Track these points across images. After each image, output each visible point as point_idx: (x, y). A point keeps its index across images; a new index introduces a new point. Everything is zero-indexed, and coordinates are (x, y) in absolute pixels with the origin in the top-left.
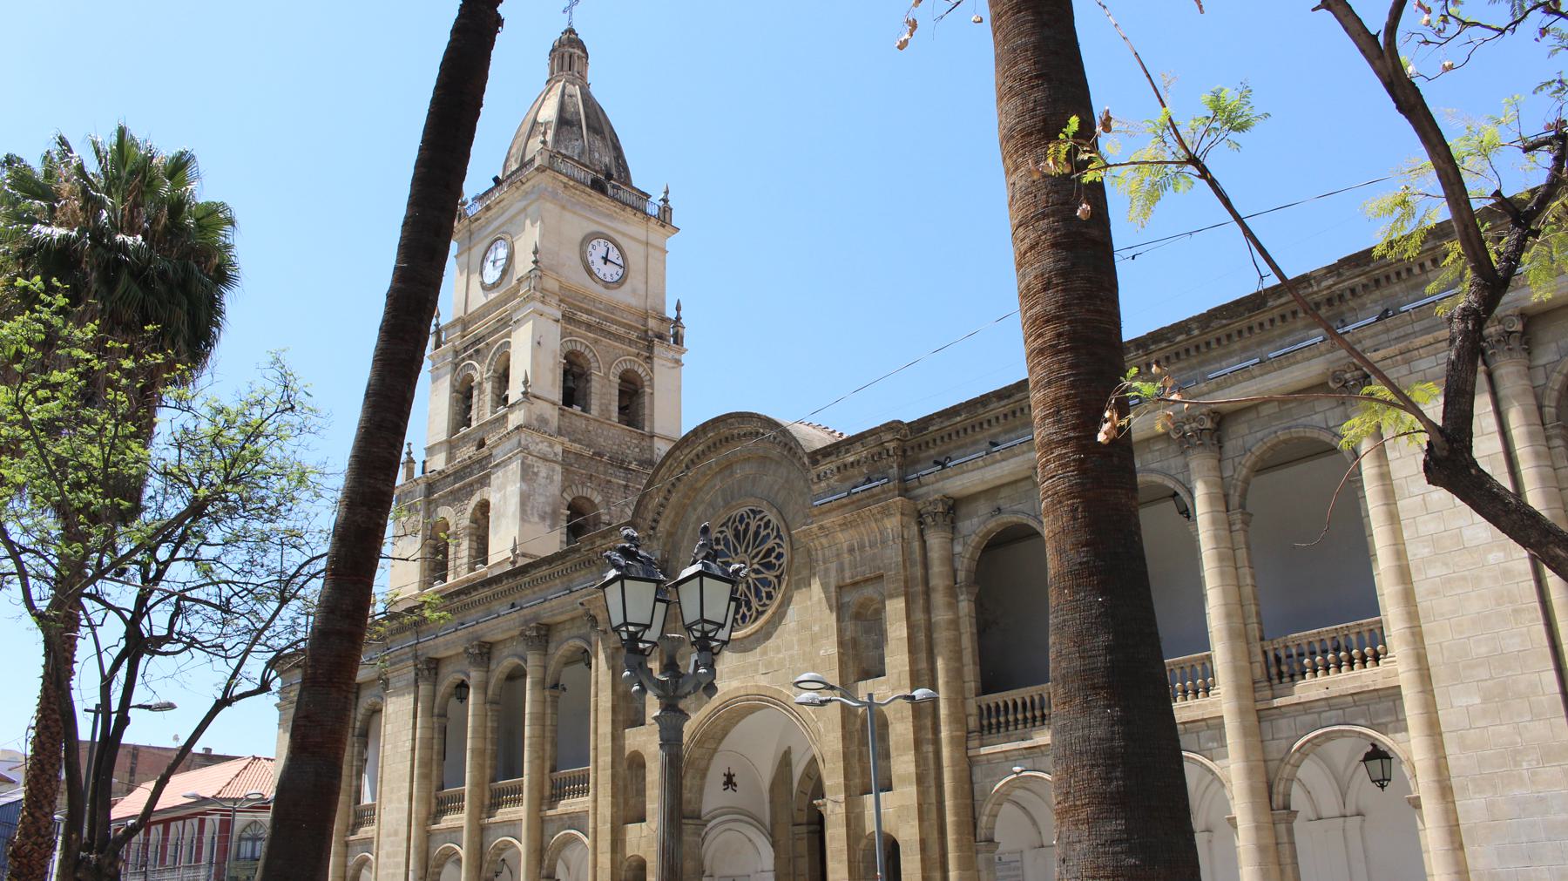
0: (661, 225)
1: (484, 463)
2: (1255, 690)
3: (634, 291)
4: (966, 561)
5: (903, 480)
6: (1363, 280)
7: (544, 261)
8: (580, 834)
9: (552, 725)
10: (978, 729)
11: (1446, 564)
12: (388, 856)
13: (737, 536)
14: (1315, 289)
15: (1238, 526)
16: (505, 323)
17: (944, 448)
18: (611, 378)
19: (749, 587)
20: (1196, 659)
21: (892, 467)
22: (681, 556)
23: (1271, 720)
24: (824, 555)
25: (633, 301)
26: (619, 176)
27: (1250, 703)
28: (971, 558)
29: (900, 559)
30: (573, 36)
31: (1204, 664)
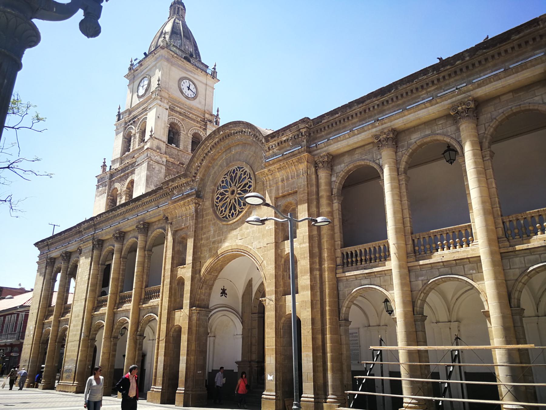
1: (133, 165)
2: (499, 242)
3: (200, 103)
4: (337, 184)
5: (308, 147)
7: (163, 85)
8: (155, 316)
9: (147, 267)
10: (342, 264)
12: (74, 327)
13: (231, 179)
14: (541, 26)
15: (487, 158)
16: (145, 110)
17: (329, 131)
18: (189, 135)
19: (235, 201)
20: (462, 227)
21: (304, 141)
22: (207, 189)
23: (509, 259)
24: (270, 184)
25: (200, 106)
26: (196, 57)
27: (496, 249)
28: (340, 183)
29: (306, 183)
31: (466, 230)
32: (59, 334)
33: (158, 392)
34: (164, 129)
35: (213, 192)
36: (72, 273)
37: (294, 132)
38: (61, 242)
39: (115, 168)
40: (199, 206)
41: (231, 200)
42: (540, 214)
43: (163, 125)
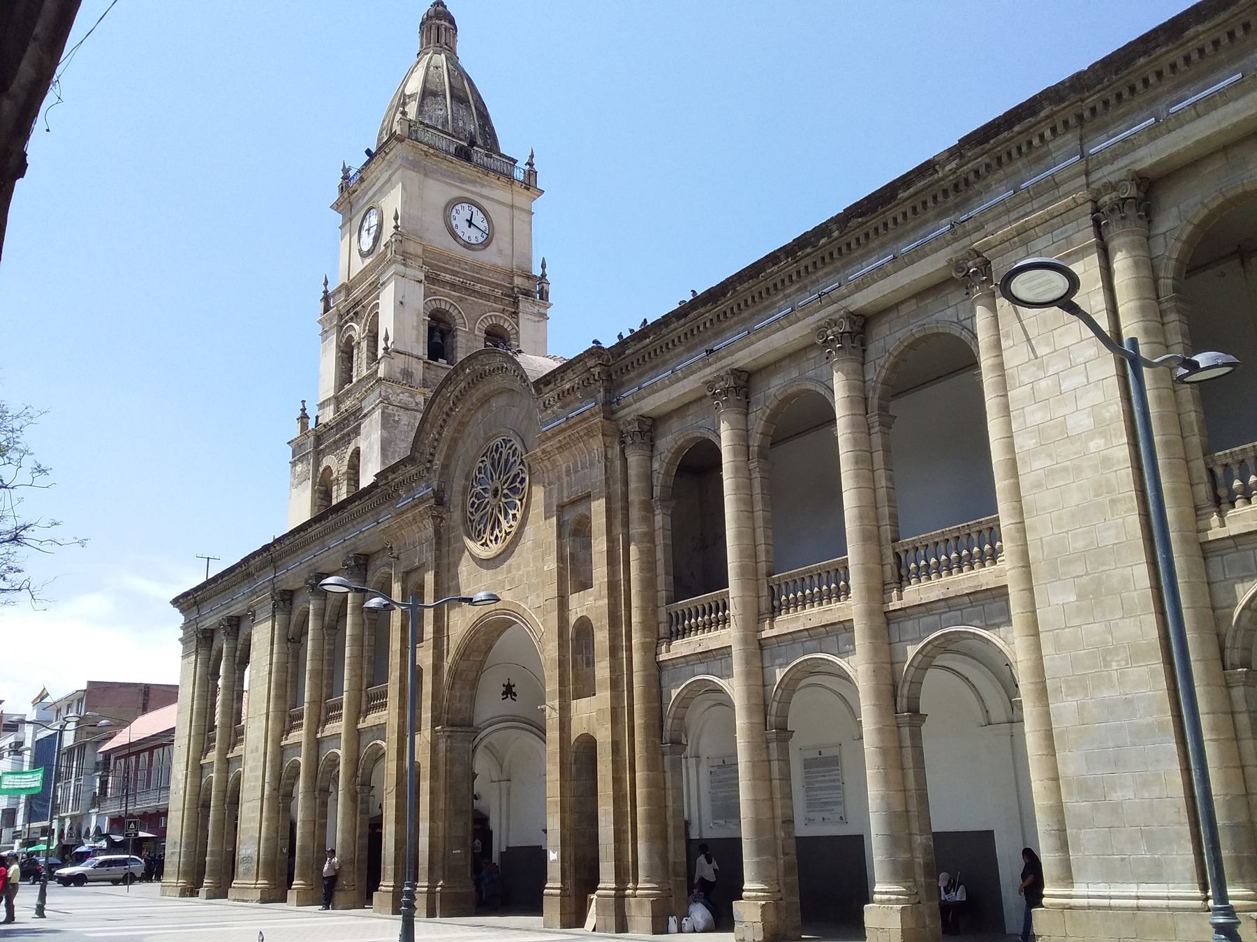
0: (525, 188)
1: (357, 414)
3: (500, 252)
4: (661, 476)
5: (608, 403)
6: (985, 159)
11: (1050, 456)
12: (251, 772)
13: (493, 465)
16: (376, 287)
18: (476, 333)
26: (485, 143)
29: (604, 478)
30: (440, 8)
32: (230, 786)
33: (387, 892)
34: (417, 328)
35: (464, 493)
36: (242, 660)
37: (580, 375)
38: (219, 596)
39: (324, 423)
40: (441, 521)
41: (493, 509)
42: (946, 537)
43: (415, 319)
